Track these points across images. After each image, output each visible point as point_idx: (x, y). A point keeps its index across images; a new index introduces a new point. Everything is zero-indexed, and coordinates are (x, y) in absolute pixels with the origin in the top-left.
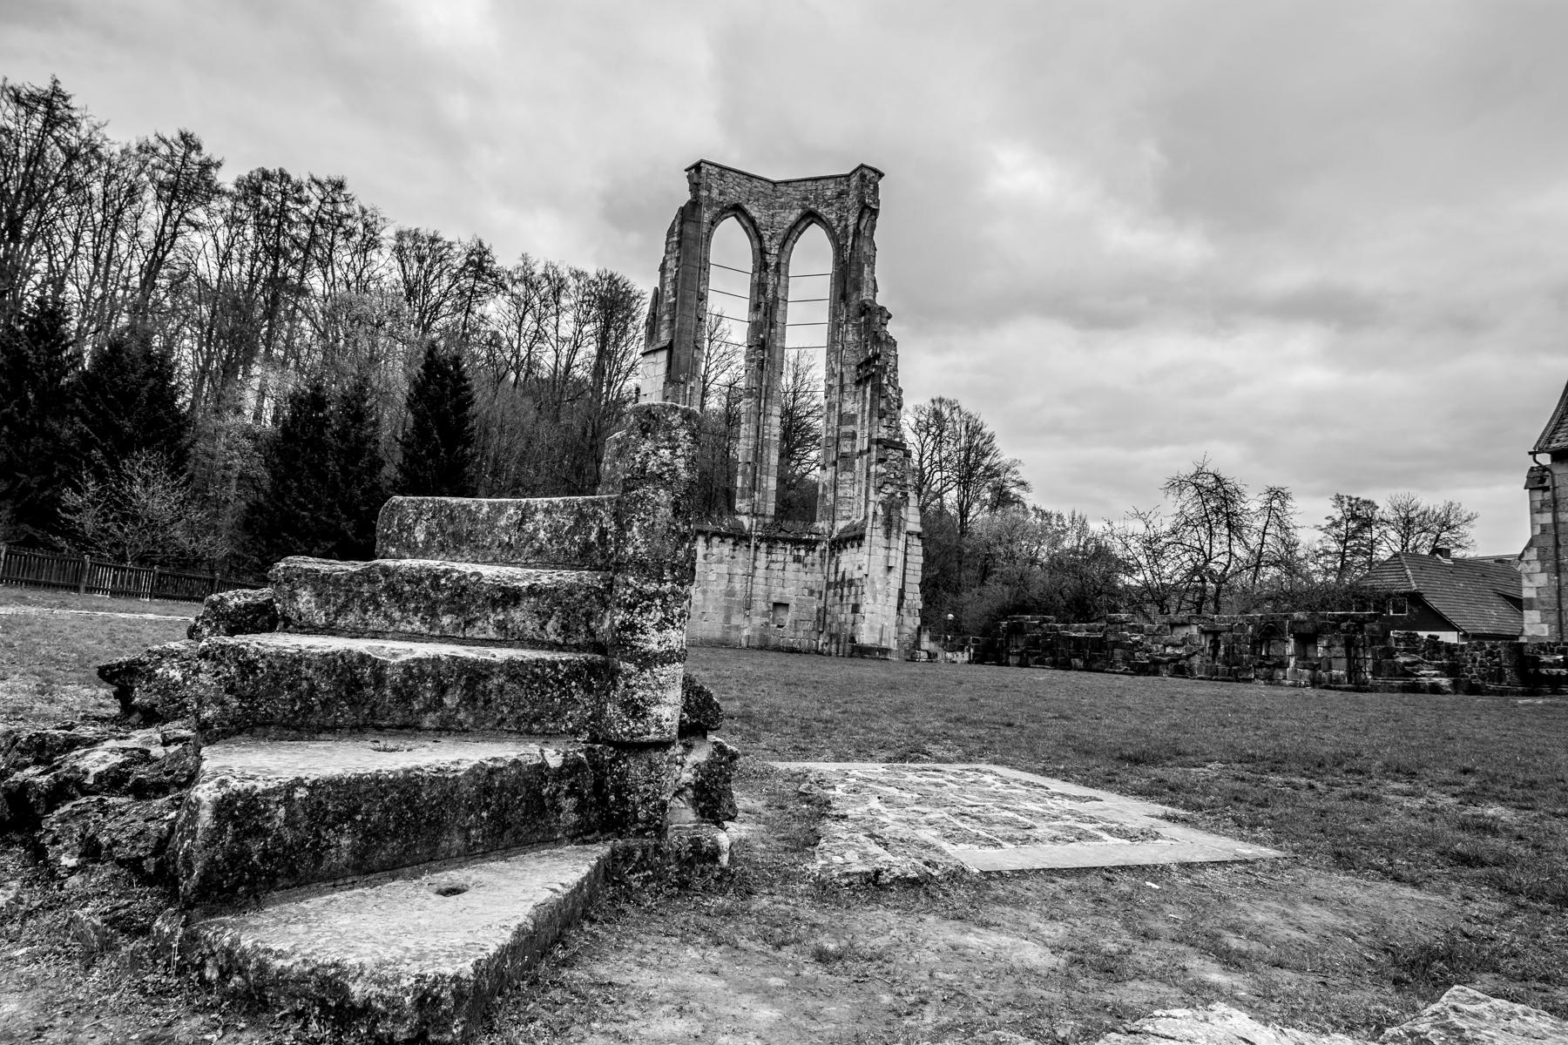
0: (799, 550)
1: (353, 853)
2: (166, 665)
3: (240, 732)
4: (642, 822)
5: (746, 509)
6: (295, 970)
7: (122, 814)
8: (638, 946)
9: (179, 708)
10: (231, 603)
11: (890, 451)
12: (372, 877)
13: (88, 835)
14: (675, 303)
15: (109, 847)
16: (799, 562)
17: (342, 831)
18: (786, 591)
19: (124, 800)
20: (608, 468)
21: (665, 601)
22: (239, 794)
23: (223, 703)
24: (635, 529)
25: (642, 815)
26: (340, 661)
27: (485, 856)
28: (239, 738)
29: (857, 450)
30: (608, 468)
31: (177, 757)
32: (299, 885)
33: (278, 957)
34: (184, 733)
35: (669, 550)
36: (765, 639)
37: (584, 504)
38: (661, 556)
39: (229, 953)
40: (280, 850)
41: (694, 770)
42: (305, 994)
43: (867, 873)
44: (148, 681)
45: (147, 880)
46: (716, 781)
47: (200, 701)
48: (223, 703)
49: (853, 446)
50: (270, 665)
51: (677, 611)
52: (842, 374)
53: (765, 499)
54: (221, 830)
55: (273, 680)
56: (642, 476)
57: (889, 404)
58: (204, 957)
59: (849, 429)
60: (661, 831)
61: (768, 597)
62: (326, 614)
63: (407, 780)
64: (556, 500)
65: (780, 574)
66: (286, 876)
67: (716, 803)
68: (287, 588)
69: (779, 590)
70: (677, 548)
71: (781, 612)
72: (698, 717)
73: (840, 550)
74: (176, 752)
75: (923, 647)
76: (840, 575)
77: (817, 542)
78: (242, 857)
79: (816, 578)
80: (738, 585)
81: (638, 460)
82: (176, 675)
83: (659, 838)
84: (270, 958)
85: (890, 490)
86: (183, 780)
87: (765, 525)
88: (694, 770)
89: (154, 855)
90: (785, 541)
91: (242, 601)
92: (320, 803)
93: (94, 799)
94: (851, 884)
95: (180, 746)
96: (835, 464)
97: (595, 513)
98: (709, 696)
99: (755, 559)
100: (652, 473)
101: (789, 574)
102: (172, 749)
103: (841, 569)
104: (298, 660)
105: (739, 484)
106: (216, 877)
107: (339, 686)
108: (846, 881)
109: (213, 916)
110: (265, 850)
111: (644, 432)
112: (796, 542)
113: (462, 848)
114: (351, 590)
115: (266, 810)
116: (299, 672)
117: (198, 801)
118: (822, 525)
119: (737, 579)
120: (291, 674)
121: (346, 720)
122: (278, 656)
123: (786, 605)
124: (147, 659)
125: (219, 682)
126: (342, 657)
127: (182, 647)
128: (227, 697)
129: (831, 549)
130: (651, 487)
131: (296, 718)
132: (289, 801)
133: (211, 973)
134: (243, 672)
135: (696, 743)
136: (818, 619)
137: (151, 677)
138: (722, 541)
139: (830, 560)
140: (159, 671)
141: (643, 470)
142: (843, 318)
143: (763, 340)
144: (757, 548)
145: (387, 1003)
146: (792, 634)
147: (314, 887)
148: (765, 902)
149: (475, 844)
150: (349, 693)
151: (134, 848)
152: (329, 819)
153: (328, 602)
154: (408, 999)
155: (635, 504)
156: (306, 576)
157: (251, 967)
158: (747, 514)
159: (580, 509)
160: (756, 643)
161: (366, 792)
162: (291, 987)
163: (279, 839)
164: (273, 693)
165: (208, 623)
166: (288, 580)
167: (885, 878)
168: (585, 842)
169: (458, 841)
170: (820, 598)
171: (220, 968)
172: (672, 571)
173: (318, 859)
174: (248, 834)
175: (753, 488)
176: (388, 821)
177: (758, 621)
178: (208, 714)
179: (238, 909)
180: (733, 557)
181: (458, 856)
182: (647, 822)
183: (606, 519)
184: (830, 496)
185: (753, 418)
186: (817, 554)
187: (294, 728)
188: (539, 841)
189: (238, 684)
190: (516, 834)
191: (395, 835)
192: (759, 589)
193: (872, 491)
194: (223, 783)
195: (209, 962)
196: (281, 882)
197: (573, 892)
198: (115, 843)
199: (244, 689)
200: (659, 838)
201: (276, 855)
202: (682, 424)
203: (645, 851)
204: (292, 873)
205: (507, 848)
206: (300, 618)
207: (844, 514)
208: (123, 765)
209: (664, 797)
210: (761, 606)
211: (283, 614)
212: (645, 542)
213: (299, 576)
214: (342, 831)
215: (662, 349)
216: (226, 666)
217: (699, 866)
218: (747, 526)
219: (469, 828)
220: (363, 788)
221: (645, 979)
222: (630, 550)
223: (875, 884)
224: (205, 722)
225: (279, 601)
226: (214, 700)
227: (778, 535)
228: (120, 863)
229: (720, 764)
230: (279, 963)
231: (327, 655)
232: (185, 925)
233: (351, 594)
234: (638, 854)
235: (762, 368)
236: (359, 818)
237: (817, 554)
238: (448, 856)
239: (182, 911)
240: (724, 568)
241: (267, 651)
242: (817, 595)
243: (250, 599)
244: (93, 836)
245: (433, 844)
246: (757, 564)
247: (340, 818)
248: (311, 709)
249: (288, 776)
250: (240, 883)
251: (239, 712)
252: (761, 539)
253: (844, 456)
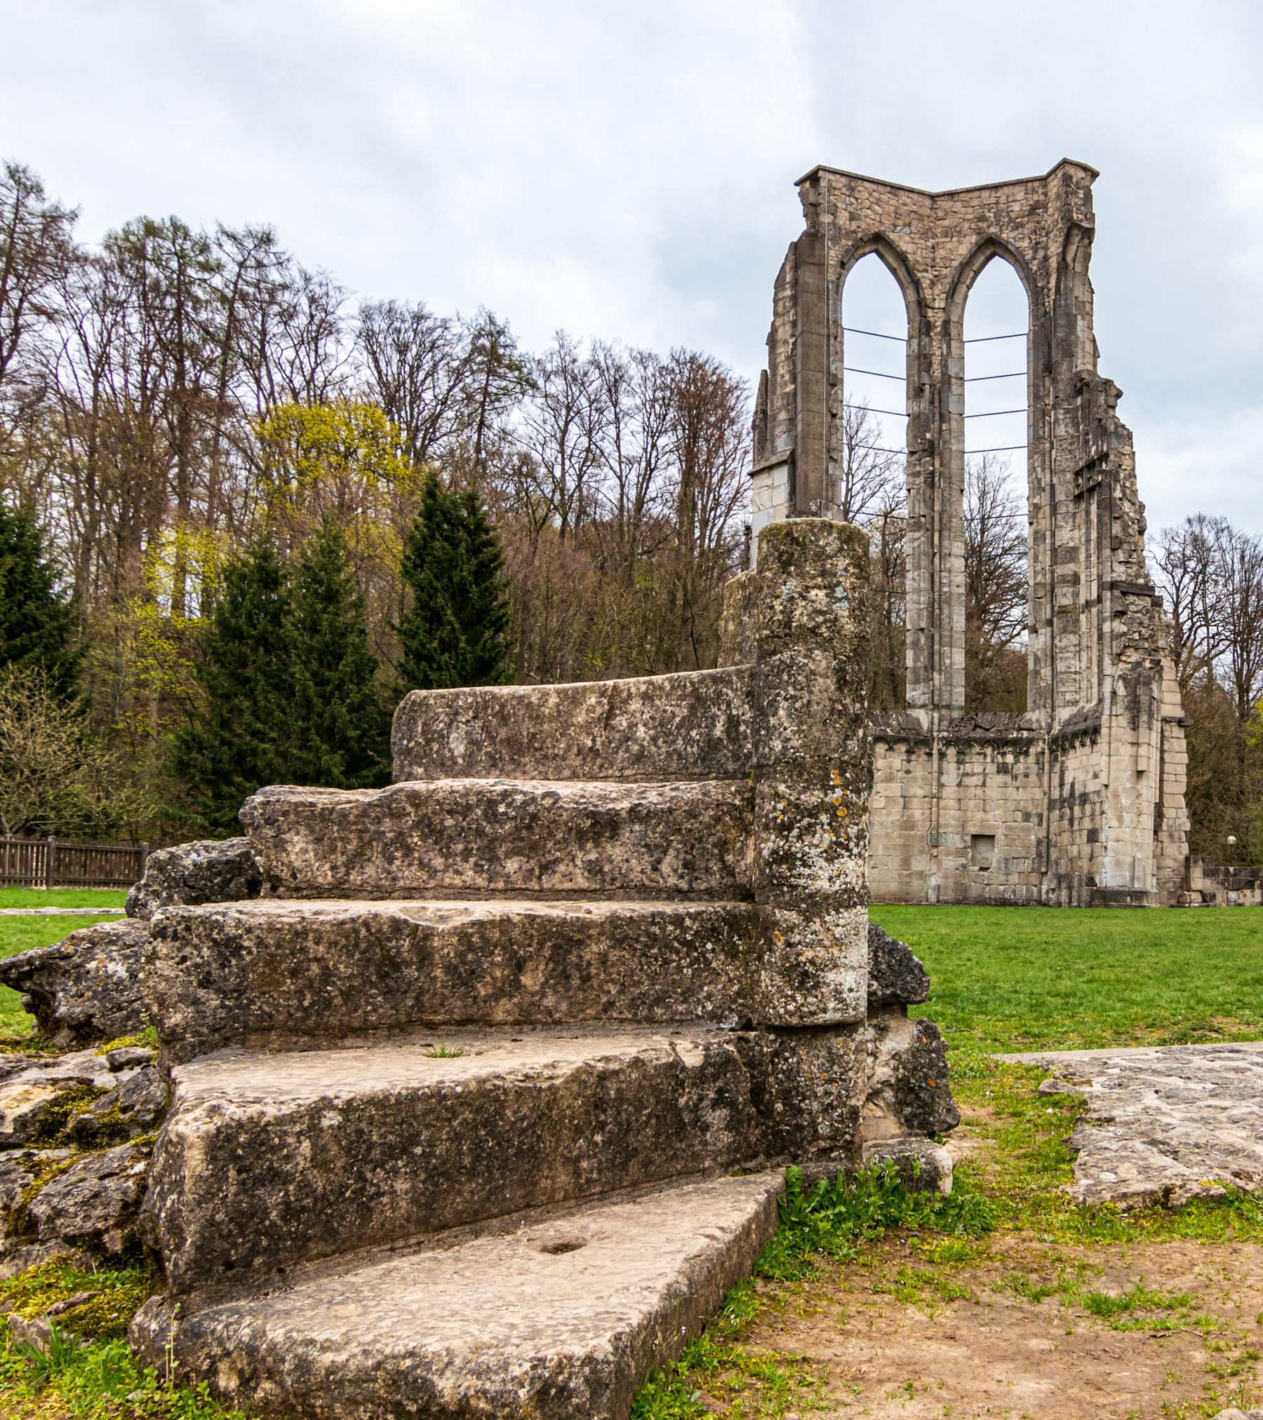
0: (1004, 754)
1: (414, 1201)
2: (101, 956)
3: (226, 1042)
4: (824, 1138)
5: (923, 699)
6: (352, 1365)
7: (64, 1171)
8: (836, 1309)
9: (128, 1018)
10: (187, 862)
11: (1131, 598)
12: (445, 1234)
13: (15, 1206)
14: (795, 394)
15: (50, 1219)
17: (395, 1171)
18: (990, 816)
19: (63, 1152)
20: (731, 627)
21: (834, 816)
22: (240, 1125)
23: (196, 1002)
24: (781, 713)
25: (823, 1129)
26: (363, 932)
27: (604, 1197)
28: (226, 1051)
29: (1082, 601)
30: (731, 627)
31: (135, 1086)
32: (342, 1252)
33: (324, 1349)
34: (140, 1051)
35: (835, 740)
36: (962, 889)
37: (700, 682)
38: (824, 751)
39: (251, 1350)
40: (308, 1202)
41: (892, 1063)
42: (372, 1398)
43: (1152, 1193)
44: (77, 981)
45: (113, 1262)
46: (926, 1077)
47: (161, 1000)
48: (196, 1002)
49: (1076, 595)
50: (261, 943)
51: (853, 831)
52: (1052, 486)
53: (949, 682)
54: (219, 1177)
55: (266, 964)
56: (786, 633)
57: (1125, 528)
58: (214, 1360)
59: (1069, 568)
60: (852, 1149)
61: (963, 827)
62: (333, 868)
63: (483, 1094)
64: (657, 679)
65: (979, 792)
66: (322, 1239)
67: (928, 1108)
68: (269, 832)
69: (979, 815)
70: (847, 738)
71: (983, 847)
72: (893, 985)
73: (1064, 751)
74: (133, 1079)
76: (1067, 788)
77: (1030, 742)
78: (253, 1215)
79: (1032, 795)
80: (917, 814)
81: (779, 608)
82: (119, 969)
83: (851, 1159)
84: (313, 1353)
85: (1134, 657)
86: (149, 1117)
87: (951, 721)
88: (892, 1063)
89: (118, 1225)
90: (984, 742)
91: (203, 858)
92: (360, 1132)
93: (18, 1153)
94: (1130, 1208)
95: (138, 1070)
96: (1050, 623)
97: (719, 694)
98: (907, 955)
99: (940, 773)
100: (800, 626)
101: (993, 792)
102: (126, 1075)
103: (1069, 778)
104: (301, 932)
105: (909, 663)
106: (219, 1245)
107: (366, 967)
108: (1123, 1205)
109: (220, 1301)
110: (287, 1204)
111: (785, 566)
112: (1000, 744)
113: (570, 1188)
114: (366, 830)
115: (283, 1145)
116: (304, 950)
117: (181, 1138)
118: (1035, 716)
119: (915, 803)
120: (292, 953)
121: (380, 1017)
122: (271, 928)
123: (991, 838)
124: (71, 950)
125: (187, 972)
126: (366, 924)
127: (122, 929)
128: (201, 993)
129: (1052, 751)
130: (801, 648)
131: (305, 1019)
132: (314, 1130)
133: (227, 1382)
134: (220, 954)
135: (893, 1024)
136: (1039, 855)
137: (80, 974)
138: (891, 749)
139: (1051, 767)
140: (92, 965)
141: (788, 624)
142: (1050, 400)
143: (931, 443)
144: (942, 755)
145: (493, 1400)
146: (1002, 878)
147: (363, 1252)
148: (1010, 1240)
149: (588, 1181)
150: (383, 977)
151: (87, 1217)
152: (376, 1154)
153: (333, 850)
154: (522, 1393)
155: (779, 675)
156: (297, 813)
157: (287, 1366)
158: (923, 706)
159: (696, 690)
160: (950, 896)
161: (426, 1113)
162: (349, 1390)
163: (305, 1186)
164: (269, 983)
165: (156, 894)
166: (270, 822)
167: (1179, 1198)
168: (746, 1171)
169: (563, 1178)
170: (1040, 824)
171: (241, 1373)
172: (842, 772)
173: (365, 1212)
174: (260, 1181)
175: (930, 667)
176: (460, 1153)
177: (950, 863)
178: (175, 1019)
179: (257, 1290)
180: (908, 772)
181: (565, 1199)
182: (832, 1138)
183: (736, 702)
184: (1046, 672)
185: (924, 562)
186: (1031, 759)
187: (305, 1033)
188: (680, 1173)
189: (216, 973)
190: (646, 1164)
191: (473, 1173)
192: (950, 817)
193: (1107, 660)
194: (215, 1110)
195: (223, 1366)
196: (314, 1248)
197: (737, 1239)
198: (59, 1213)
199: (225, 979)
200: (851, 1159)
201: (304, 1209)
202: (841, 549)
203: (833, 1178)
204: (330, 1233)
205: (635, 1184)
206: (294, 876)
207: (1068, 697)
208: (55, 1102)
209: (853, 1102)
210: (953, 840)
211: (268, 871)
212: (799, 731)
213: (285, 814)
214: (395, 1171)
215: (779, 464)
216: (195, 947)
217: (910, 1197)
218: (925, 724)
219: (578, 1159)
220: (420, 1107)
221: (854, 1350)
222: (777, 745)
223: (1164, 1206)
224: (173, 1032)
225: (260, 853)
226: (183, 998)
227: (973, 735)
228: (71, 1240)
229: (930, 1052)
230: (327, 1358)
231: (343, 923)
232: (181, 1317)
233: (366, 836)
234: (823, 1183)
235: (932, 485)
236: (418, 1150)
237: (1031, 759)
238: (551, 1200)
239: (174, 1298)
240: (895, 789)
241: (253, 922)
242: (1036, 820)
243: (214, 854)
244: (24, 1206)
245: (530, 1182)
246: (944, 779)
247: (391, 1152)
248: (328, 1003)
249: (309, 1096)
250: (254, 1252)
251: (222, 1013)
252: (948, 743)
253: (1063, 611)
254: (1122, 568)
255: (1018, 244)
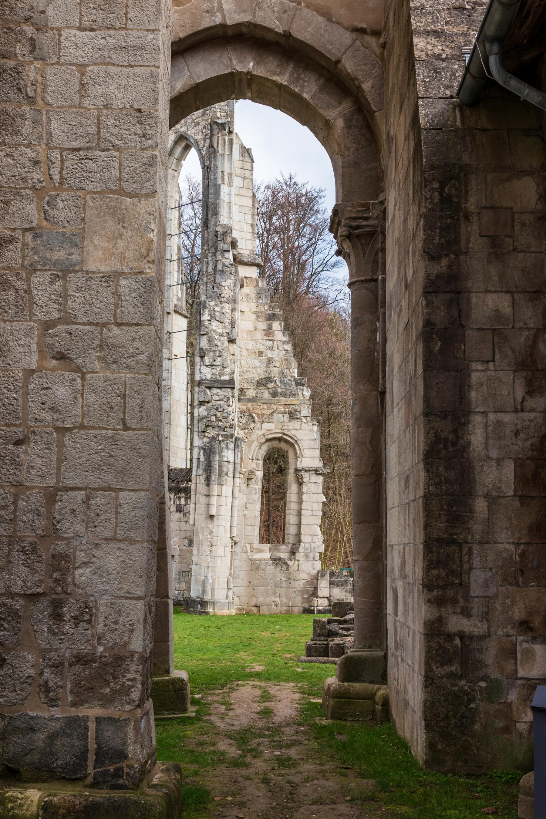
0: (180, 498)
11: (215, 391)
16: (181, 511)
75: (320, 593)
193: (196, 437)
254: (209, 369)
255: (196, 138)
